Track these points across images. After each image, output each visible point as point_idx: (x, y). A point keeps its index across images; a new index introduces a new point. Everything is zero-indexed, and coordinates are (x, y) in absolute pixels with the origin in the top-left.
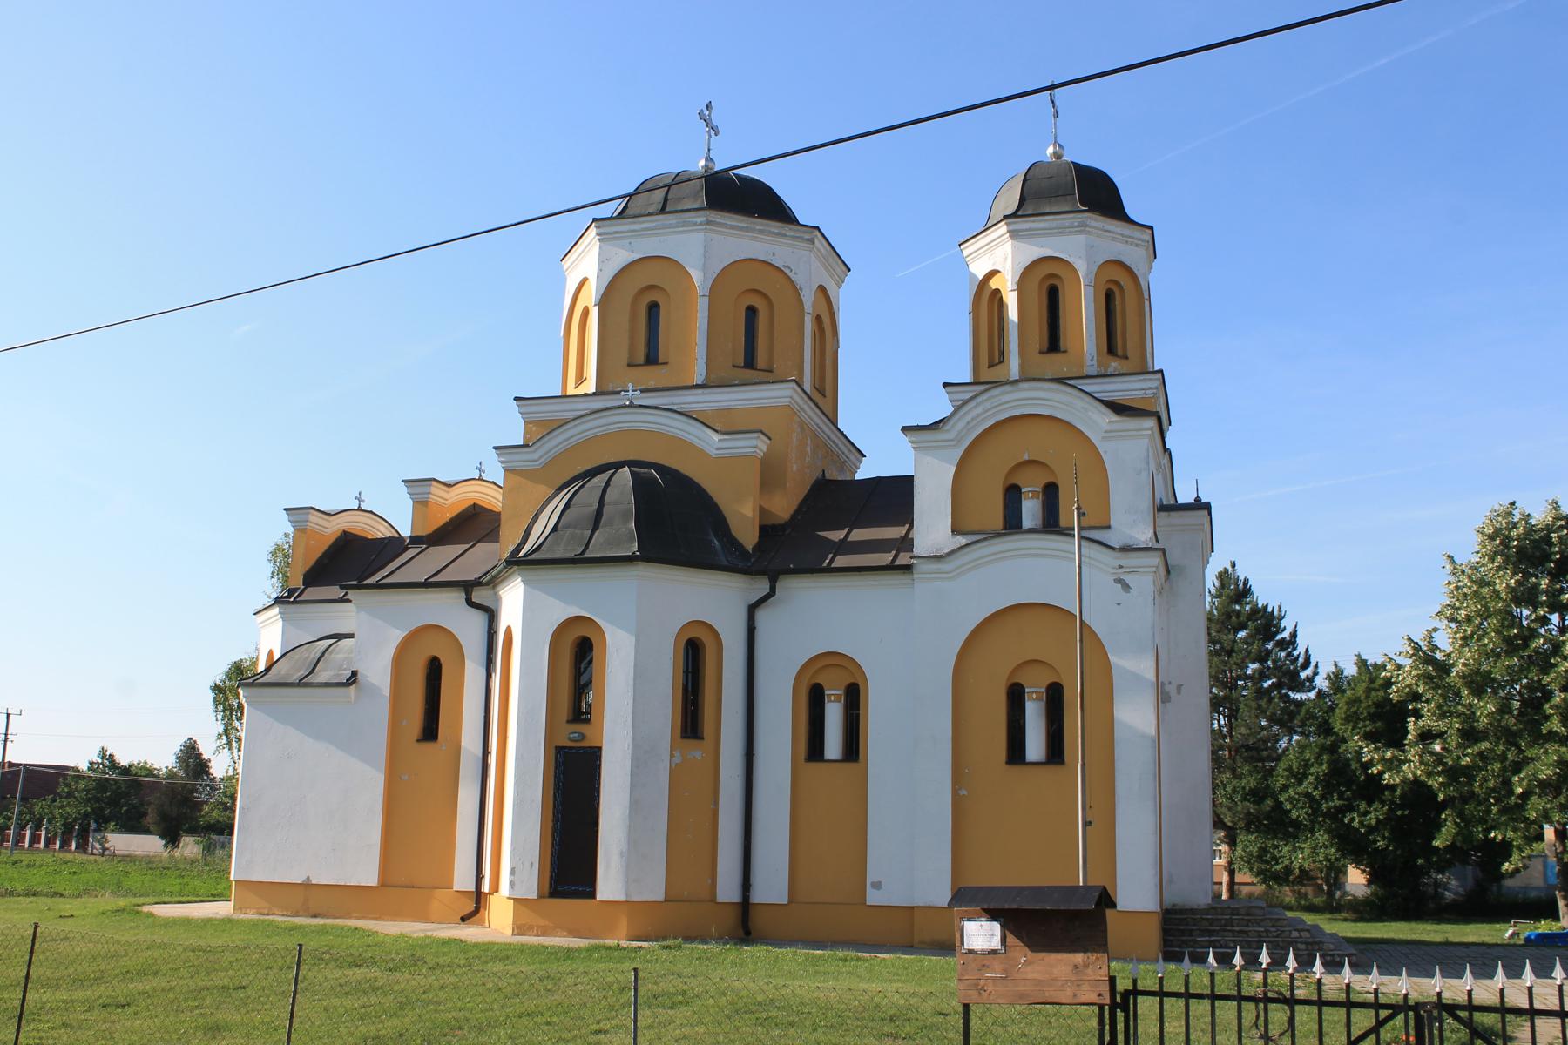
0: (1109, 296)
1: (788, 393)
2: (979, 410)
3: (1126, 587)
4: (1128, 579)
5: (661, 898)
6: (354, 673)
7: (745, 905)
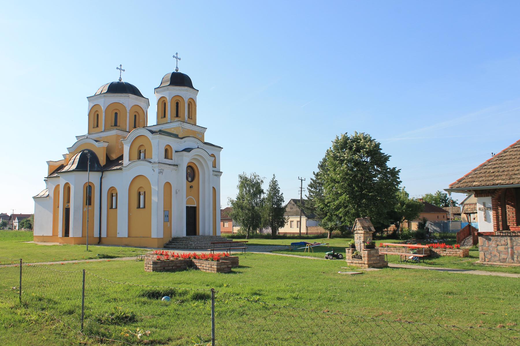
0: (177, 104)
7: (100, 238)
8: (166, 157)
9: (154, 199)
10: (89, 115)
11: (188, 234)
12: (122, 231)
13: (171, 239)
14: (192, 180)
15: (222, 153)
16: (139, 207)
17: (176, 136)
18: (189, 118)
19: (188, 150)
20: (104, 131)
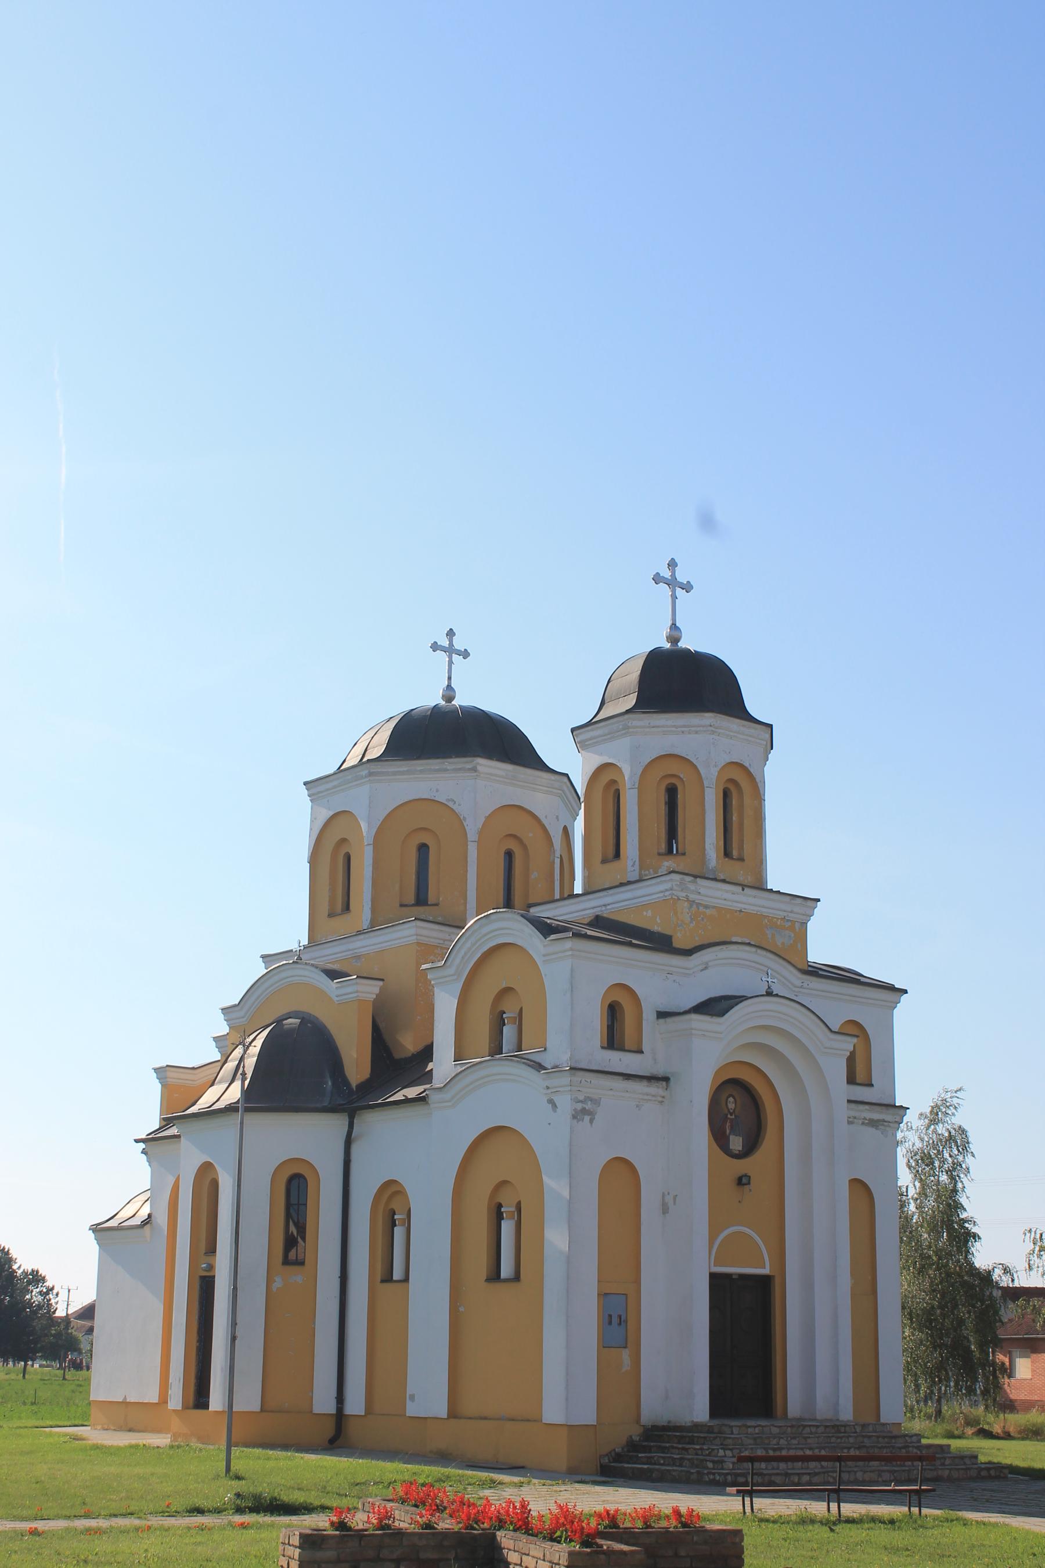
0: (672, 793)
1: (412, 931)
2: (468, 945)
3: (554, 1106)
4: (556, 1099)
5: (257, 1407)
6: (150, 1216)
7: (340, 1416)
8: (613, 1040)
9: (556, 1238)
10: (314, 860)
11: (714, 1413)
12: (427, 1393)
13: (635, 1432)
14: (751, 1147)
15: (903, 1014)
16: (494, 1276)
17: (660, 943)
18: (727, 854)
19: (715, 1006)
20: (375, 925)
